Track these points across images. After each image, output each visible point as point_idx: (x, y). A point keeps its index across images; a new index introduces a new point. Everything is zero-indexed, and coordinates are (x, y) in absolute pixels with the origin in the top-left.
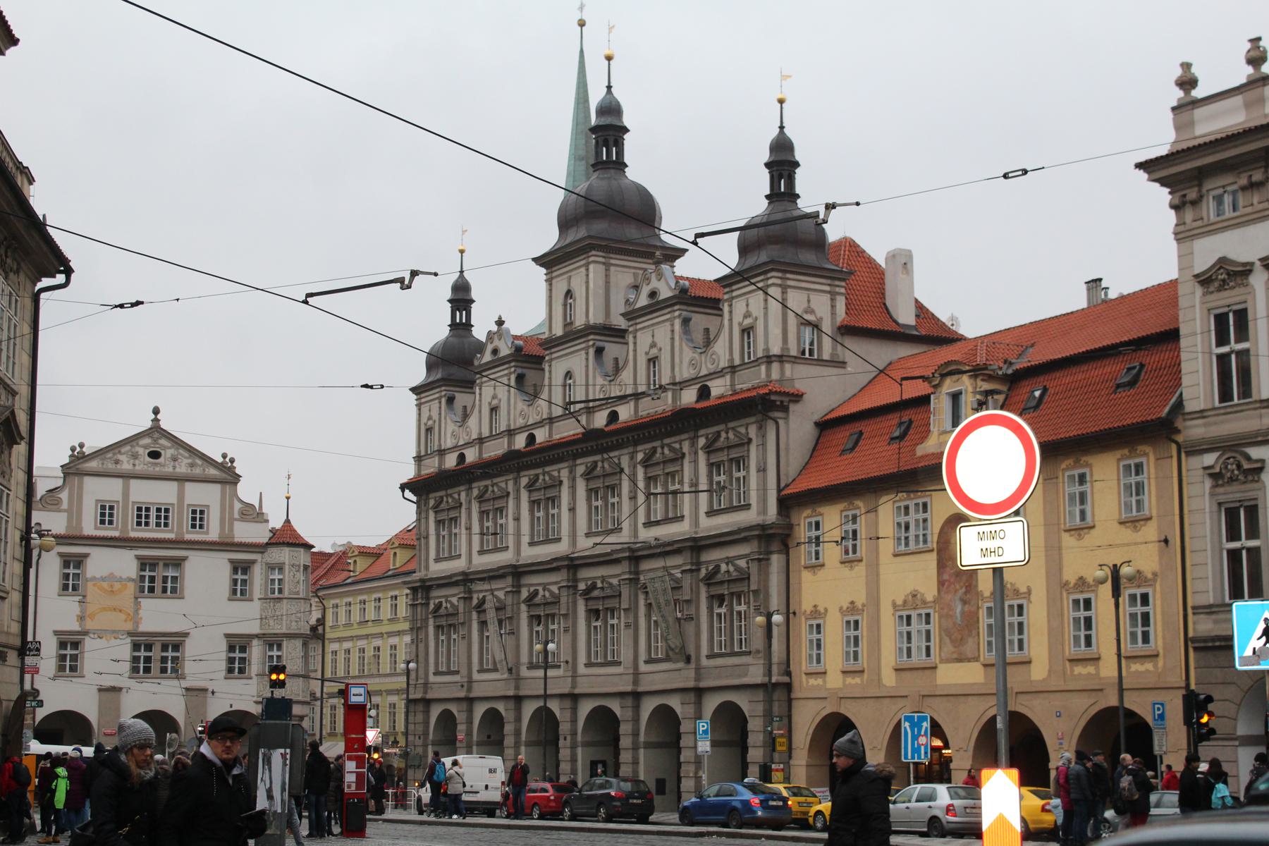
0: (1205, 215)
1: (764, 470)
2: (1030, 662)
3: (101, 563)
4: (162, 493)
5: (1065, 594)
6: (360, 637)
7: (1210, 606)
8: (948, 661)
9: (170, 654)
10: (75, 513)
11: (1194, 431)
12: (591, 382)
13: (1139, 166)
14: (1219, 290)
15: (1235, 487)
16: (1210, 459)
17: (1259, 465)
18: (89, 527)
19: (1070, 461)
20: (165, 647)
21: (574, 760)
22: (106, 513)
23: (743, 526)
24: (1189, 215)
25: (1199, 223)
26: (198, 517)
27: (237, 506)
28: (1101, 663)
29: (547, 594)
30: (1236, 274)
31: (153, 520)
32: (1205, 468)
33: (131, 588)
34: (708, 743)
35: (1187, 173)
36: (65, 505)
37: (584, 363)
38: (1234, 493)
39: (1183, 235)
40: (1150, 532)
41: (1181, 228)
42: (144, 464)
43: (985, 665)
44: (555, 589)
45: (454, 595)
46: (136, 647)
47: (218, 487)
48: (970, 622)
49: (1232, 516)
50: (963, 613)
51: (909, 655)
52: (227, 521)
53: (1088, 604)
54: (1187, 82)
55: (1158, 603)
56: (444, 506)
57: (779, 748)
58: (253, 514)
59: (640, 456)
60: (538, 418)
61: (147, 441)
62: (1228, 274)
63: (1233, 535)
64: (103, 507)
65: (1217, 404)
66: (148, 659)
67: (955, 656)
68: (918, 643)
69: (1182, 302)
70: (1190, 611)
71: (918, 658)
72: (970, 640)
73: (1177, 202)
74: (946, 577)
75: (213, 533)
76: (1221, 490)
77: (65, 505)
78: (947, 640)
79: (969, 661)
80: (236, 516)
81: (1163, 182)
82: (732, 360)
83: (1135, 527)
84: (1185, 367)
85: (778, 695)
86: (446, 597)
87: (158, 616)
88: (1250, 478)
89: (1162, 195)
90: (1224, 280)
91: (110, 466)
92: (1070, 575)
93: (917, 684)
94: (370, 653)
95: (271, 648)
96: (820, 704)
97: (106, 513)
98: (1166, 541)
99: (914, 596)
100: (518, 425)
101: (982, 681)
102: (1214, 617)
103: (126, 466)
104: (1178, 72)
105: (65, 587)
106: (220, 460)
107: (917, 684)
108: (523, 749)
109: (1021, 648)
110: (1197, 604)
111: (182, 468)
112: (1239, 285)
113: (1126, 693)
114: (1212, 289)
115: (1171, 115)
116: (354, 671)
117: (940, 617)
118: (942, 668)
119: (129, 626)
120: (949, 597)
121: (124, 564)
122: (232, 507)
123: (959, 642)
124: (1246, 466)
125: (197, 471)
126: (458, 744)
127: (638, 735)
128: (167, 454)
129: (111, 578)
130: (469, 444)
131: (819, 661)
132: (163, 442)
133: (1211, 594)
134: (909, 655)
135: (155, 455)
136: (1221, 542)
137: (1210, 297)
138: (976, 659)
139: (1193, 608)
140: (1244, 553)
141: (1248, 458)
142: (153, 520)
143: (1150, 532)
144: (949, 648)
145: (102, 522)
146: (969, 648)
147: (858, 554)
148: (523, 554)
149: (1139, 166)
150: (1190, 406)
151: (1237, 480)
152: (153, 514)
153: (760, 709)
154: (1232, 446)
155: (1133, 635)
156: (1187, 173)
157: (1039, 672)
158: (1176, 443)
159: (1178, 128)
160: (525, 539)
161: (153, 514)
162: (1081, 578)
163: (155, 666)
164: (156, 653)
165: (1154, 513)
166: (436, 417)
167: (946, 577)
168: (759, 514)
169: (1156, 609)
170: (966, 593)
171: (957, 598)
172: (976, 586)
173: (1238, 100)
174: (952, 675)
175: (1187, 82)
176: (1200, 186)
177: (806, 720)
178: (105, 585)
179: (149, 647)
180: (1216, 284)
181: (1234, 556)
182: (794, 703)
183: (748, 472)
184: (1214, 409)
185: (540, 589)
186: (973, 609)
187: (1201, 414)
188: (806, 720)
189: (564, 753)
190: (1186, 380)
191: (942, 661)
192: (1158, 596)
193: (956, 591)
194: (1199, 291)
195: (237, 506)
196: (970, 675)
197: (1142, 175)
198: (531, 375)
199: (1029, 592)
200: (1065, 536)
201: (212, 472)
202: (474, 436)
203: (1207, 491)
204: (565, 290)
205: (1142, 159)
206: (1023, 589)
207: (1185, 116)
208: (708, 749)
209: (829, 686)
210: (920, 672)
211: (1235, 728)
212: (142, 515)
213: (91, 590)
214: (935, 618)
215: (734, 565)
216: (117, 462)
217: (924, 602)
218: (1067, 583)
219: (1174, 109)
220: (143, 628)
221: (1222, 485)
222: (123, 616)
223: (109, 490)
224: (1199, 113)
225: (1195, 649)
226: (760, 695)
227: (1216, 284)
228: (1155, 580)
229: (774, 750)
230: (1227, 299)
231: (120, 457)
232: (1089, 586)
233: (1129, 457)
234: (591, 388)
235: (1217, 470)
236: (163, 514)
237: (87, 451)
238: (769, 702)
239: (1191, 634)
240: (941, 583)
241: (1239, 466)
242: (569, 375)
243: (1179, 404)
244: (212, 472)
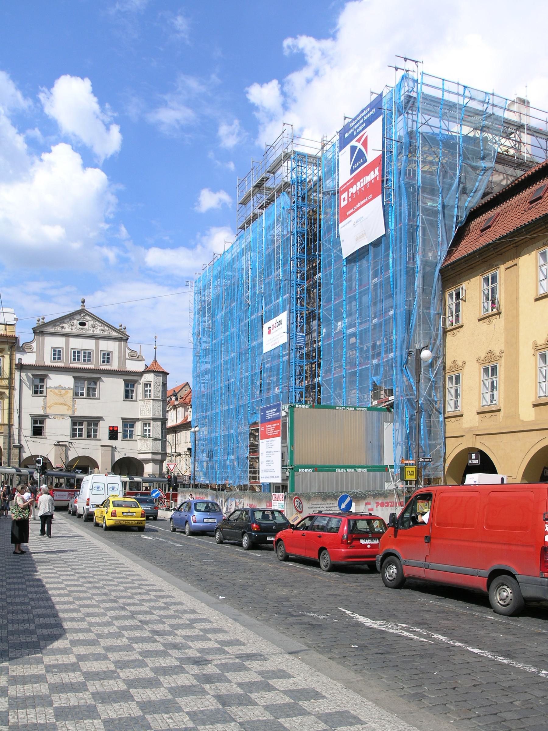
3: (54, 381)
4: (88, 344)
9: (92, 427)
10: (40, 353)
18: (48, 362)
20: (89, 425)
22: (57, 354)
26: (107, 357)
27: (128, 351)
31: (82, 358)
33: (71, 393)
36: (35, 350)
42: (76, 329)
46: (74, 423)
47: (117, 343)
52: (122, 359)
58: (135, 357)
61: (78, 317)
64: (55, 351)
66: (81, 430)
75: (115, 366)
77: (35, 350)
80: (127, 357)
87: (85, 408)
91: (58, 329)
95: (146, 426)
97: (57, 354)
103: (67, 329)
105: (36, 392)
106: (118, 328)
111: (98, 332)
119: (70, 413)
121: (68, 381)
122: (125, 352)
125: (106, 333)
128: (90, 323)
129: (59, 387)
132: (87, 318)
135: (82, 324)
142: (82, 358)
145: (55, 358)
152: (82, 355)
161: (82, 355)
163: (85, 433)
164: (84, 427)
178: (56, 391)
179: (81, 424)
195: (128, 351)
199: (464, 363)
201: (114, 334)
212: (76, 354)
213: (50, 394)
216: (63, 328)
220: (77, 414)
222: (66, 407)
223: (59, 342)
231: (64, 325)
236: (88, 355)
237: (46, 321)
244: (114, 334)
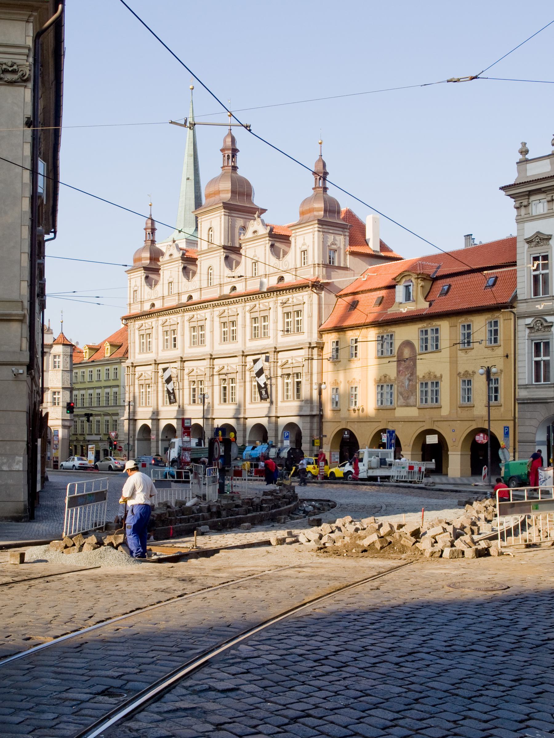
0: (530, 212)
1: (158, 339)
2: (441, 407)
5: (458, 378)
6: (89, 388)
7: (526, 385)
8: (401, 406)
11: (521, 308)
12: (180, 281)
13: (502, 188)
14: (535, 246)
15: (539, 333)
16: (529, 321)
17: (551, 324)
19: (463, 319)
21: (157, 447)
23: (301, 342)
24: (523, 211)
25: (528, 216)
28: (442, 409)
29: (229, 368)
30: (544, 239)
32: (526, 325)
34: (288, 441)
35: (522, 193)
37: (263, 252)
38: (539, 336)
39: (520, 220)
40: (500, 352)
41: (519, 217)
43: (419, 409)
44: (149, 373)
45: (149, 370)
48: (412, 390)
49: (537, 346)
50: (409, 385)
51: (426, 402)
53: (469, 382)
54: (524, 152)
55: (502, 383)
56: (143, 328)
57: (316, 444)
59: (248, 308)
60: (194, 288)
62: (540, 239)
63: (537, 354)
65: (533, 297)
67: (404, 404)
68: (386, 397)
69: (519, 251)
70: (517, 387)
71: (387, 404)
72: (412, 397)
73: (518, 205)
74: (401, 369)
76: (533, 334)
78: (401, 397)
79: (411, 406)
81: (511, 196)
82: (296, 265)
83: (466, 352)
84: (519, 280)
85: (316, 420)
86: (145, 371)
88: (546, 330)
89: (511, 202)
90: (538, 242)
92: (461, 370)
93: (387, 415)
94: (95, 396)
96: (421, 424)
98: (507, 356)
99: (385, 377)
100: (183, 291)
101: (417, 415)
102: (528, 390)
104: (520, 146)
107: (387, 415)
108: (136, 442)
109: (437, 401)
110: (520, 384)
112: (545, 245)
113: (491, 422)
114: (532, 246)
115: (516, 166)
116: (95, 404)
117: (398, 386)
118: (397, 409)
120: (402, 378)
123: (406, 398)
124: (545, 324)
126: (152, 440)
127: (277, 437)
130: (194, 291)
131: (437, 401)
133: (527, 380)
134: (426, 402)
136: (532, 358)
137: (531, 249)
138: (415, 406)
139: (518, 385)
140: (542, 362)
141: (546, 321)
143: (500, 352)
144: (401, 400)
146: (411, 401)
147: (393, 353)
148: (160, 355)
149: (502, 188)
150: (520, 297)
151: (541, 330)
153: (308, 426)
154: (539, 316)
155: (422, 399)
156: (522, 193)
157: (445, 411)
158: (514, 313)
159: (519, 171)
160: (248, 336)
162: (466, 371)
165: (502, 344)
166: (139, 284)
167: (401, 369)
168: (308, 337)
169: (501, 385)
170: (410, 376)
171: (406, 378)
172: (416, 373)
173: (548, 161)
174: (401, 412)
175: (524, 152)
176: (529, 199)
177: (330, 431)
180: (534, 243)
181: (537, 363)
182: (324, 424)
183: (303, 317)
184: (531, 299)
185: (195, 369)
186: (414, 383)
187: (525, 301)
188: (330, 431)
189: (153, 444)
190: (519, 286)
191: (398, 406)
192: (502, 380)
193: (406, 375)
194: (526, 246)
196: (413, 412)
197: (503, 193)
198: (233, 256)
199: (441, 376)
200: (459, 352)
202: (198, 287)
203: (527, 335)
204: (209, 227)
205: (503, 185)
206: (438, 375)
207: (522, 166)
208: (289, 444)
209: (342, 416)
210: (436, 410)
211: (535, 437)
214: (395, 387)
215: (295, 360)
217: (390, 380)
218: (460, 373)
219: (517, 163)
221: (534, 333)
224: (529, 166)
225: (518, 403)
226: (308, 419)
227: (534, 243)
228: (501, 373)
229: (313, 445)
230: (539, 251)
232: (470, 375)
233: (464, 322)
234: (180, 284)
235: (532, 326)
238: (312, 423)
239: (517, 397)
240: (399, 372)
241: (542, 324)
242: (210, 268)
243: (515, 297)
